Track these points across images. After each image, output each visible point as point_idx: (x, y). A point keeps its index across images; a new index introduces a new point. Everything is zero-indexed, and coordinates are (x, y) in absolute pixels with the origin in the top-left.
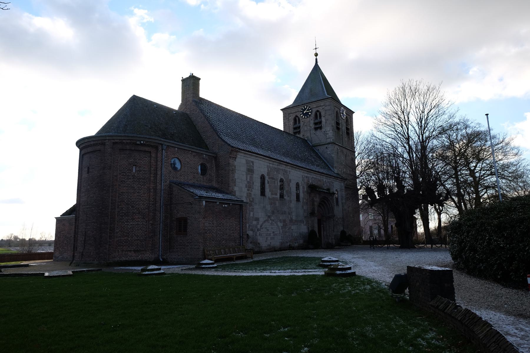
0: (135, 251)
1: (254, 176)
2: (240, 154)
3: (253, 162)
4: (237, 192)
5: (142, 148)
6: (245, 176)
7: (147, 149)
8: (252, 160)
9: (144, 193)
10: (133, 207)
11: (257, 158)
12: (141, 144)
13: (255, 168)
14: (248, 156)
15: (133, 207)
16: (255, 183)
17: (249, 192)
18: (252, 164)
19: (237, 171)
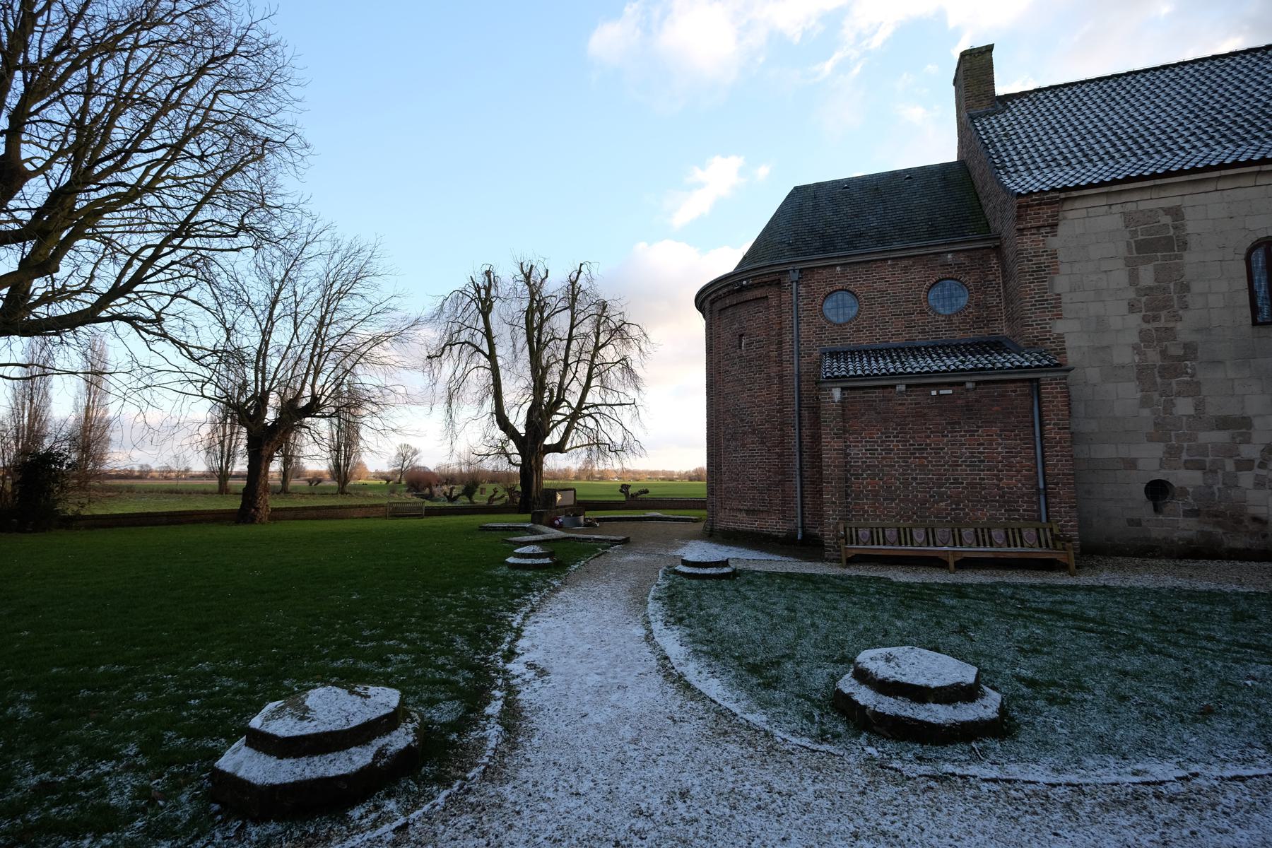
0: (748, 512)
1: (1190, 257)
2: (1078, 204)
3: (1176, 213)
4: (1070, 342)
5: (749, 295)
6: (1120, 277)
7: (758, 293)
8: (1176, 202)
9: (761, 389)
10: (742, 420)
11: (1203, 188)
12: (746, 287)
13: (1191, 227)
14: (1136, 197)
15: (742, 420)
16: (1196, 287)
17: (1162, 324)
18: (1167, 220)
19: (1064, 268)
